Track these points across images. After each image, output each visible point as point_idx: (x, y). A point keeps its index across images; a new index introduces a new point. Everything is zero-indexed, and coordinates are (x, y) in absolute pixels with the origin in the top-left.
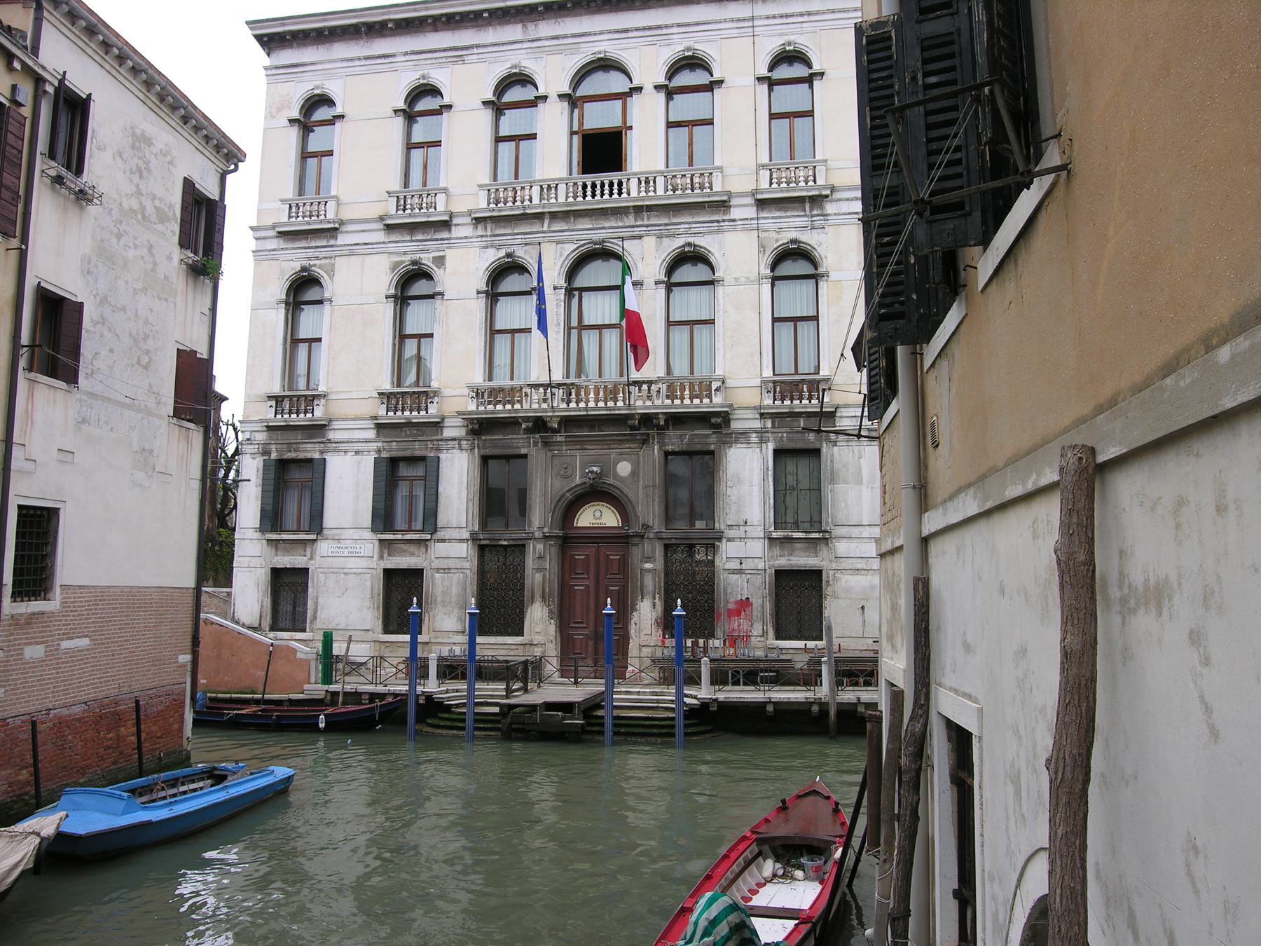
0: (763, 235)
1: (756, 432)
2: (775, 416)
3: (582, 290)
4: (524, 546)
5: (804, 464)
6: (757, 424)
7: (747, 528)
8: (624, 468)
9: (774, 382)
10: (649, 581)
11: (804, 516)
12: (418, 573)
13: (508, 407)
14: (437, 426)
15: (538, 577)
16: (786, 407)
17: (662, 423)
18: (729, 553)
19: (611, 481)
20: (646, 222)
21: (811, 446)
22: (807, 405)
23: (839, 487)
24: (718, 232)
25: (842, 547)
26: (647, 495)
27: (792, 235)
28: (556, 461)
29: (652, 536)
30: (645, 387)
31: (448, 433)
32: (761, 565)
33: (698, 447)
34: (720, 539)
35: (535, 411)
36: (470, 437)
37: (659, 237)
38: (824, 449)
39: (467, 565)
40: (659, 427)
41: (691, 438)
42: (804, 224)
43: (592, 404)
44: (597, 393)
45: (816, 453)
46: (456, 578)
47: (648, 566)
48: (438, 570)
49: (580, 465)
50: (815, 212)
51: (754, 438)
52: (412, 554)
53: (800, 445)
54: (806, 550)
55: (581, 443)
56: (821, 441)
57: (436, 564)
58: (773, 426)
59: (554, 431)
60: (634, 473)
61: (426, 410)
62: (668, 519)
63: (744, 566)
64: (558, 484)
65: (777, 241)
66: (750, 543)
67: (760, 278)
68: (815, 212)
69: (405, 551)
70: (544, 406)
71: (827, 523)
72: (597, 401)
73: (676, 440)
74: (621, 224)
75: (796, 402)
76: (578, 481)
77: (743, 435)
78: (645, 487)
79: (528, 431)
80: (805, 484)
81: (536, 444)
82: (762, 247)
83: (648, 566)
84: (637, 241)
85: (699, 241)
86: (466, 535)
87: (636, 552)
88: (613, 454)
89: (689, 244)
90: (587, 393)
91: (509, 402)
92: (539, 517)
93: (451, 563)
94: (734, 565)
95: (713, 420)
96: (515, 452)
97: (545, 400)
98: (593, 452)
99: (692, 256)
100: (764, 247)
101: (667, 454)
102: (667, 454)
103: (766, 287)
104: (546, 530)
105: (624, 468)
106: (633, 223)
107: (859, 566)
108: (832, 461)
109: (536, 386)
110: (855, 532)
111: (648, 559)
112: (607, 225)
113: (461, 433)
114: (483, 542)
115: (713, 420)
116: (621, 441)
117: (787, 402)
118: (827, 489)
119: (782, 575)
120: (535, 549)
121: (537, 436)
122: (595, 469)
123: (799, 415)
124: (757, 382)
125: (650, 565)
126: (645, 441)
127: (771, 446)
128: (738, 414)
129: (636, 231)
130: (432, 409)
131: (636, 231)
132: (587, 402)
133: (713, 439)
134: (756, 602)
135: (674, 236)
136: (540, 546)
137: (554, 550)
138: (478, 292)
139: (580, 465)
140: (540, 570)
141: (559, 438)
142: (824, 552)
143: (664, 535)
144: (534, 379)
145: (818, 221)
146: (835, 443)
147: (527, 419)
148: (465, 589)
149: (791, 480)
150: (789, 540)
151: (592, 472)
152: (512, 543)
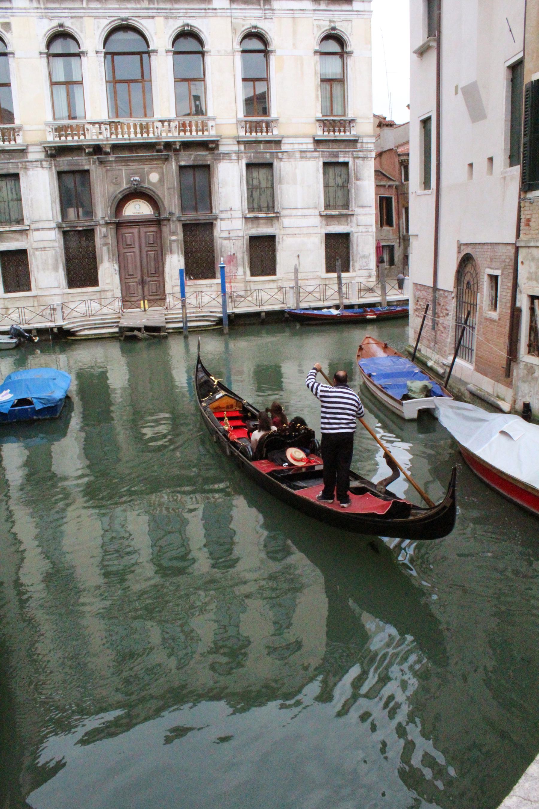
0: (234, 21)
1: (235, 153)
2: (246, 143)
3: (113, 54)
4: (93, 230)
5: (263, 173)
6: (235, 148)
7: (232, 212)
8: (154, 177)
9: (246, 122)
10: (175, 246)
11: (264, 204)
12: (24, 252)
13: (76, 138)
14: (23, 152)
15: (105, 249)
16: (253, 137)
17: (178, 147)
18: (221, 229)
19: (146, 185)
20: (156, 6)
21: (267, 161)
22: (262, 136)
23: (284, 187)
24: (205, 17)
25: (286, 222)
26: (170, 194)
27: (254, 23)
28: (109, 174)
29: (175, 219)
30: (166, 124)
31: (31, 157)
32: (241, 234)
33: (200, 163)
34: (216, 219)
35: (94, 140)
36: (49, 159)
37: (166, 18)
38: (276, 163)
39: (56, 244)
40: (176, 150)
41: (196, 156)
42: (260, 15)
43: (132, 136)
44: (135, 128)
45: (270, 165)
46: (50, 253)
47: (174, 238)
48: (37, 249)
49: (124, 176)
50: (266, 7)
51: (234, 156)
52: (17, 240)
53: (261, 161)
54: (266, 224)
55: (126, 161)
56: (272, 158)
57: (35, 245)
58: (245, 149)
59: (108, 154)
60: (161, 180)
61: (15, 141)
62: (183, 209)
63: (231, 235)
64: (112, 188)
65: (243, 26)
66: (234, 221)
67: (234, 52)
68: (266, 7)
69: (12, 238)
70: (101, 137)
71: (278, 208)
72: (136, 133)
73: (187, 158)
74: (139, 6)
75: (259, 134)
76: (125, 186)
77: (227, 155)
78: (169, 189)
79: (90, 154)
80: (264, 185)
81: (94, 163)
82: (234, 30)
83: (174, 238)
84: (151, 20)
85: (191, 22)
86: (53, 225)
87: (165, 230)
88: (146, 168)
89: (188, 25)
90: (129, 128)
91: (76, 134)
92: (102, 211)
93: (46, 244)
94: (225, 235)
95: (210, 146)
96: (81, 168)
97: (101, 133)
98: (134, 167)
99: (187, 34)
100: (235, 29)
101: (181, 168)
102: (181, 168)
103: (238, 57)
104: (107, 219)
105: (154, 177)
106: (147, 6)
107: (296, 232)
108: (280, 171)
109: (93, 123)
110: (294, 212)
111: (174, 233)
112: (129, 6)
113: (42, 156)
114: (65, 229)
115: (210, 146)
116: (151, 159)
117: (254, 134)
118: (277, 186)
119: (253, 239)
120: (100, 232)
121: (95, 157)
122: (137, 178)
123: (260, 142)
124: (234, 121)
125: (175, 236)
126: (167, 159)
127: (244, 162)
128: (223, 141)
129: (151, 13)
130: (19, 140)
131: (151, 13)
132: (129, 134)
133: (209, 157)
134: (239, 256)
135: (176, 18)
136: (104, 230)
137: (113, 232)
138: (41, 53)
139: (124, 176)
140: (106, 244)
141: (111, 158)
142: (276, 224)
143: (182, 219)
144: (89, 118)
145: (269, 14)
146: (281, 159)
147: (89, 146)
148: (56, 260)
149: (255, 182)
150: (257, 218)
151: (135, 181)
152: (85, 228)
